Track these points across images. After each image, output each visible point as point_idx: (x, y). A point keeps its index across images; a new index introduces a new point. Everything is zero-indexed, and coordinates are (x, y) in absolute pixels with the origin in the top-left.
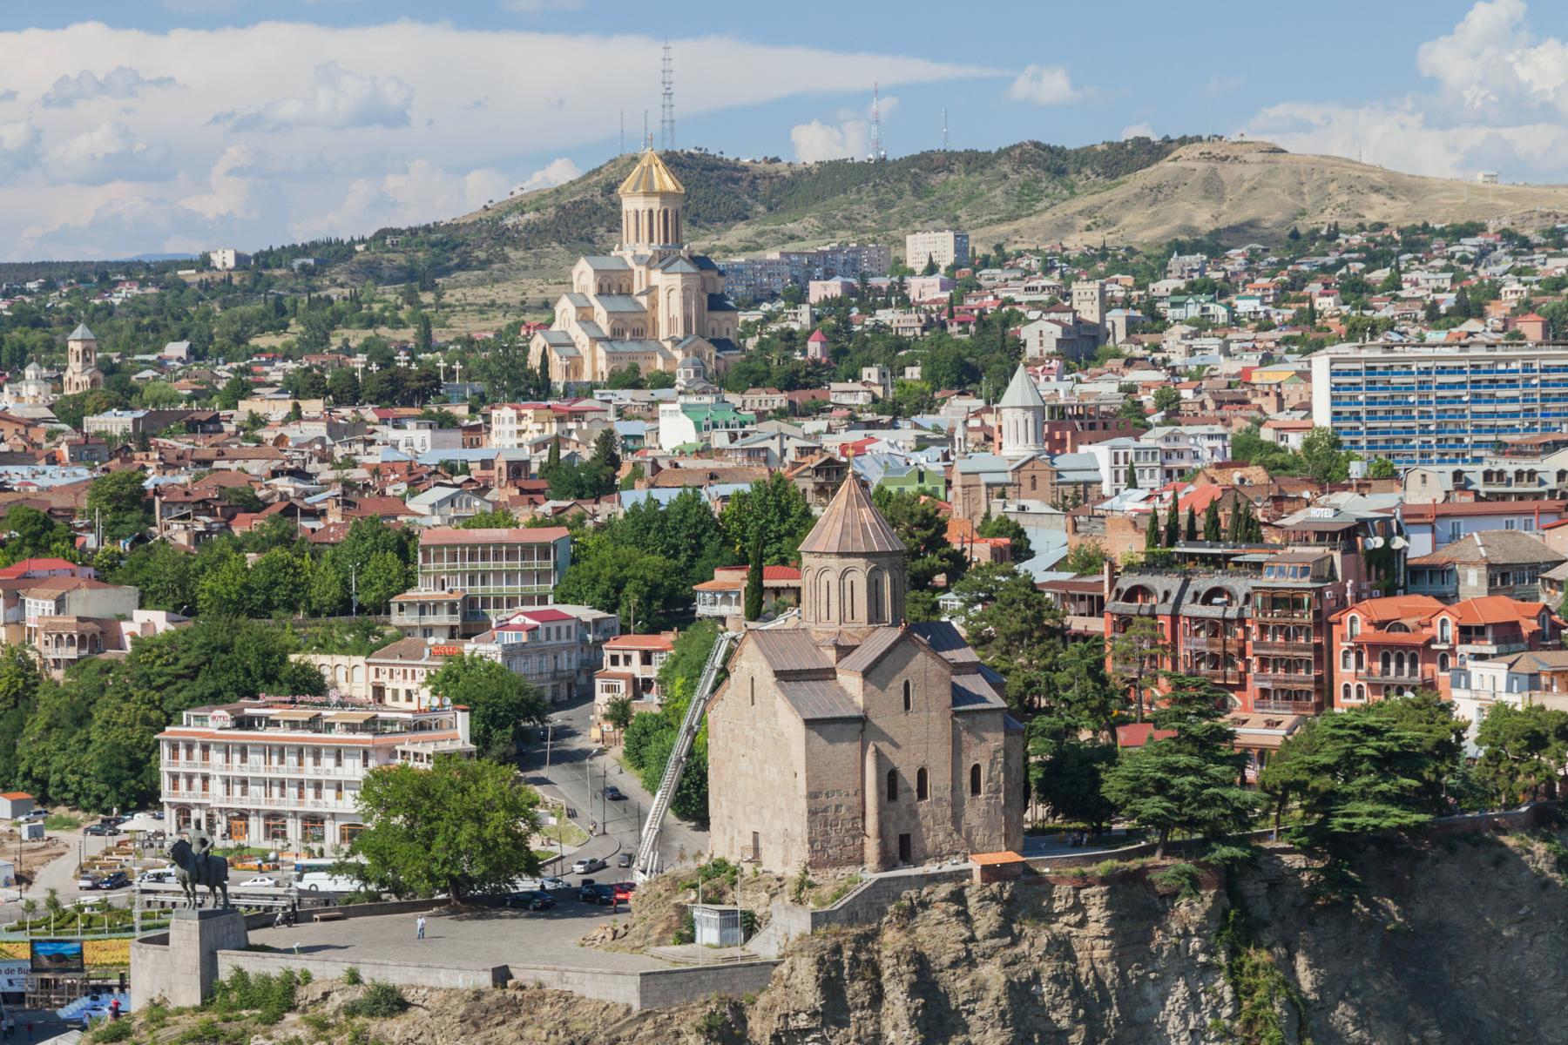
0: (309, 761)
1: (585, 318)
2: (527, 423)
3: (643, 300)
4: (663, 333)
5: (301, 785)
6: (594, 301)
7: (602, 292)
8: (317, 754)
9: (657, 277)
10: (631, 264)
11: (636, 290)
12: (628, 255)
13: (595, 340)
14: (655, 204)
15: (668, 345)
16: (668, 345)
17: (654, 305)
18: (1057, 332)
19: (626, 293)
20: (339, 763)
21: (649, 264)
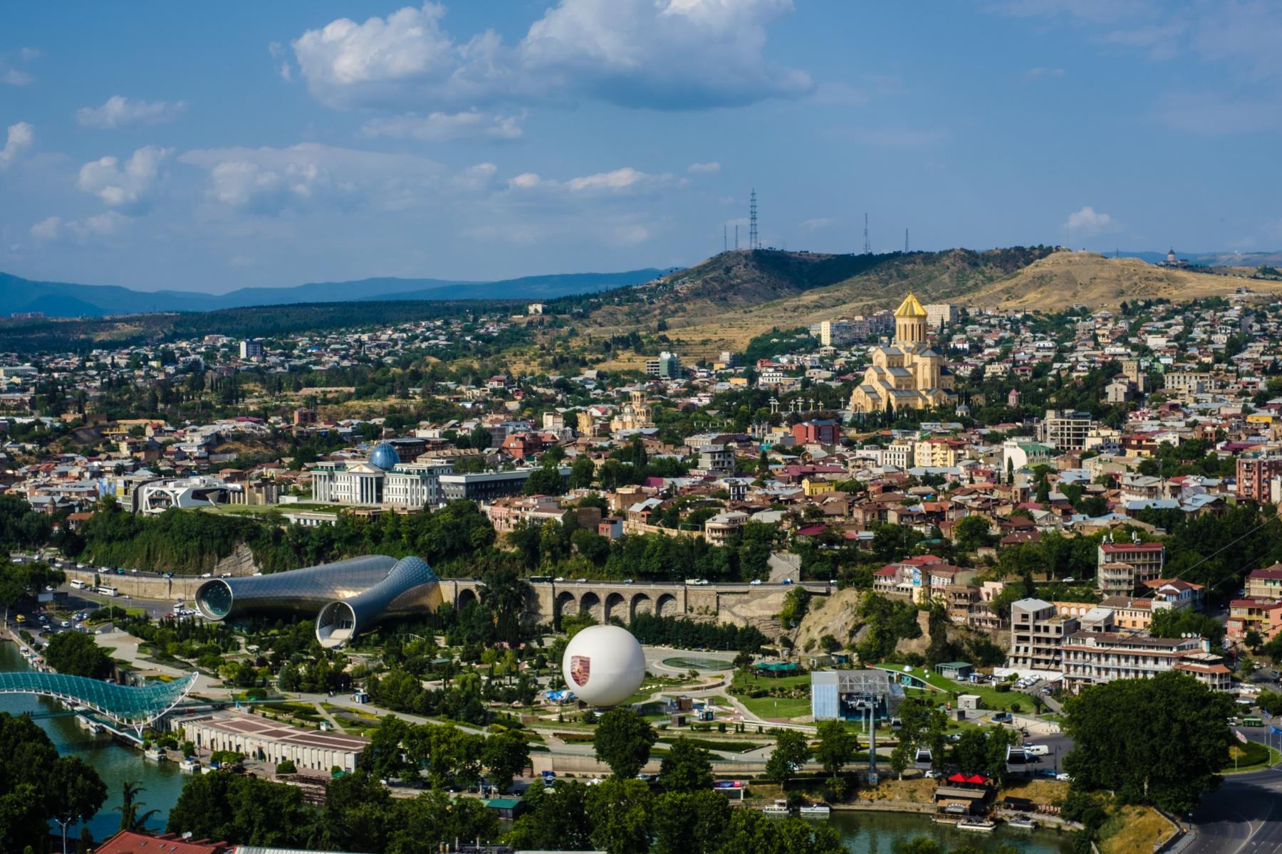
1: (882, 380)
2: (937, 450)
3: (911, 370)
4: (920, 386)
6: (886, 370)
7: (889, 367)
9: (917, 358)
10: (903, 351)
11: (906, 365)
12: (902, 349)
13: (890, 390)
14: (915, 321)
15: (924, 393)
16: (924, 393)
17: (915, 372)
18: (1125, 389)
19: (901, 367)
21: (913, 352)
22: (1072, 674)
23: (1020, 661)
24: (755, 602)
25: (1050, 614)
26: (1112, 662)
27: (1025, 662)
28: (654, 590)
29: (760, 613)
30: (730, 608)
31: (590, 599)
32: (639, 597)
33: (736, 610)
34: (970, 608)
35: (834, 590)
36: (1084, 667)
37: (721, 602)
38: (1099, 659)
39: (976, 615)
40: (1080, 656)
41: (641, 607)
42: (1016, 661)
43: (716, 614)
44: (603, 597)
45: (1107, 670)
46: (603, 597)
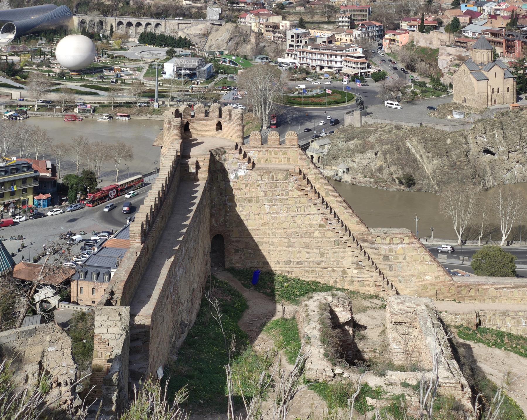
0: (329, 56)
5: (328, 61)
8: (331, 55)
20: (336, 57)
22: (302, 61)
23: (290, 55)
24: (193, 28)
25: (304, 35)
26: (318, 56)
27: (292, 56)
28: (154, 22)
29: (194, 32)
30: (183, 30)
31: (129, 24)
32: (148, 24)
33: (185, 31)
34: (273, 32)
35: (224, 23)
36: (307, 58)
37: (180, 27)
38: (328, 57)
39: (276, 35)
40: (305, 53)
41: (149, 29)
42: (288, 55)
43: (177, 33)
44: (134, 24)
45: (331, 61)
46: (134, 24)
